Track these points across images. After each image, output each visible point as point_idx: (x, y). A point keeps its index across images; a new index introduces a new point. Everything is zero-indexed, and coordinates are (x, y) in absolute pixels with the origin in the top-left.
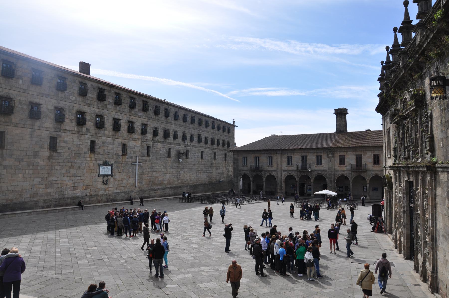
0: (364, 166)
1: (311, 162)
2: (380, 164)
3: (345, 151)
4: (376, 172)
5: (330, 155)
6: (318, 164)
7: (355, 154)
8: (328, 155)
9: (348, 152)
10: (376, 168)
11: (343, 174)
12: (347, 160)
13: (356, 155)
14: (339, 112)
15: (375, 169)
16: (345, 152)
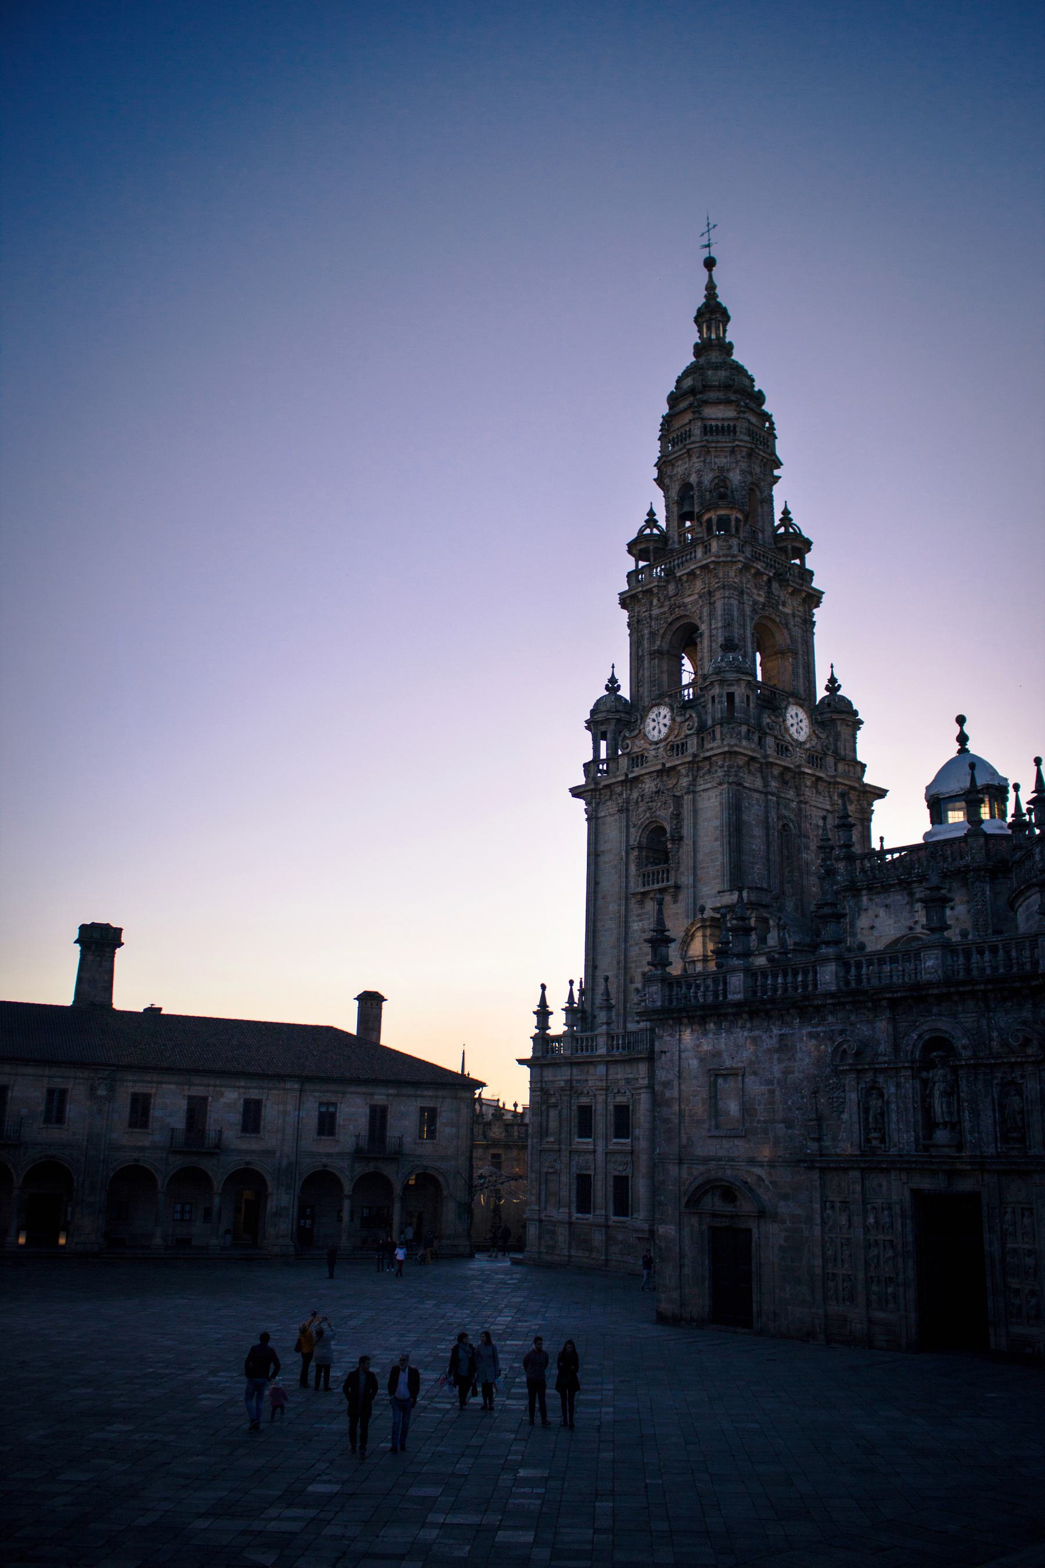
0: (212, 1134)
1: (24, 1112)
2: (262, 1130)
3: (155, 1079)
4: (248, 1159)
5: (102, 1092)
6: (47, 1120)
7: (186, 1093)
8: (93, 1089)
9: (164, 1086)
10: (250, 1144)
11: (137, 1160)
12: (156, 1113)
13: (190, 1098)
14: (96, 935)
15: (244, 1146)
16: (155, 1085)
